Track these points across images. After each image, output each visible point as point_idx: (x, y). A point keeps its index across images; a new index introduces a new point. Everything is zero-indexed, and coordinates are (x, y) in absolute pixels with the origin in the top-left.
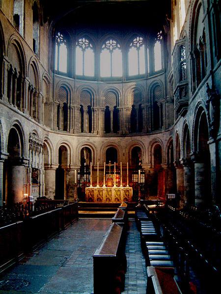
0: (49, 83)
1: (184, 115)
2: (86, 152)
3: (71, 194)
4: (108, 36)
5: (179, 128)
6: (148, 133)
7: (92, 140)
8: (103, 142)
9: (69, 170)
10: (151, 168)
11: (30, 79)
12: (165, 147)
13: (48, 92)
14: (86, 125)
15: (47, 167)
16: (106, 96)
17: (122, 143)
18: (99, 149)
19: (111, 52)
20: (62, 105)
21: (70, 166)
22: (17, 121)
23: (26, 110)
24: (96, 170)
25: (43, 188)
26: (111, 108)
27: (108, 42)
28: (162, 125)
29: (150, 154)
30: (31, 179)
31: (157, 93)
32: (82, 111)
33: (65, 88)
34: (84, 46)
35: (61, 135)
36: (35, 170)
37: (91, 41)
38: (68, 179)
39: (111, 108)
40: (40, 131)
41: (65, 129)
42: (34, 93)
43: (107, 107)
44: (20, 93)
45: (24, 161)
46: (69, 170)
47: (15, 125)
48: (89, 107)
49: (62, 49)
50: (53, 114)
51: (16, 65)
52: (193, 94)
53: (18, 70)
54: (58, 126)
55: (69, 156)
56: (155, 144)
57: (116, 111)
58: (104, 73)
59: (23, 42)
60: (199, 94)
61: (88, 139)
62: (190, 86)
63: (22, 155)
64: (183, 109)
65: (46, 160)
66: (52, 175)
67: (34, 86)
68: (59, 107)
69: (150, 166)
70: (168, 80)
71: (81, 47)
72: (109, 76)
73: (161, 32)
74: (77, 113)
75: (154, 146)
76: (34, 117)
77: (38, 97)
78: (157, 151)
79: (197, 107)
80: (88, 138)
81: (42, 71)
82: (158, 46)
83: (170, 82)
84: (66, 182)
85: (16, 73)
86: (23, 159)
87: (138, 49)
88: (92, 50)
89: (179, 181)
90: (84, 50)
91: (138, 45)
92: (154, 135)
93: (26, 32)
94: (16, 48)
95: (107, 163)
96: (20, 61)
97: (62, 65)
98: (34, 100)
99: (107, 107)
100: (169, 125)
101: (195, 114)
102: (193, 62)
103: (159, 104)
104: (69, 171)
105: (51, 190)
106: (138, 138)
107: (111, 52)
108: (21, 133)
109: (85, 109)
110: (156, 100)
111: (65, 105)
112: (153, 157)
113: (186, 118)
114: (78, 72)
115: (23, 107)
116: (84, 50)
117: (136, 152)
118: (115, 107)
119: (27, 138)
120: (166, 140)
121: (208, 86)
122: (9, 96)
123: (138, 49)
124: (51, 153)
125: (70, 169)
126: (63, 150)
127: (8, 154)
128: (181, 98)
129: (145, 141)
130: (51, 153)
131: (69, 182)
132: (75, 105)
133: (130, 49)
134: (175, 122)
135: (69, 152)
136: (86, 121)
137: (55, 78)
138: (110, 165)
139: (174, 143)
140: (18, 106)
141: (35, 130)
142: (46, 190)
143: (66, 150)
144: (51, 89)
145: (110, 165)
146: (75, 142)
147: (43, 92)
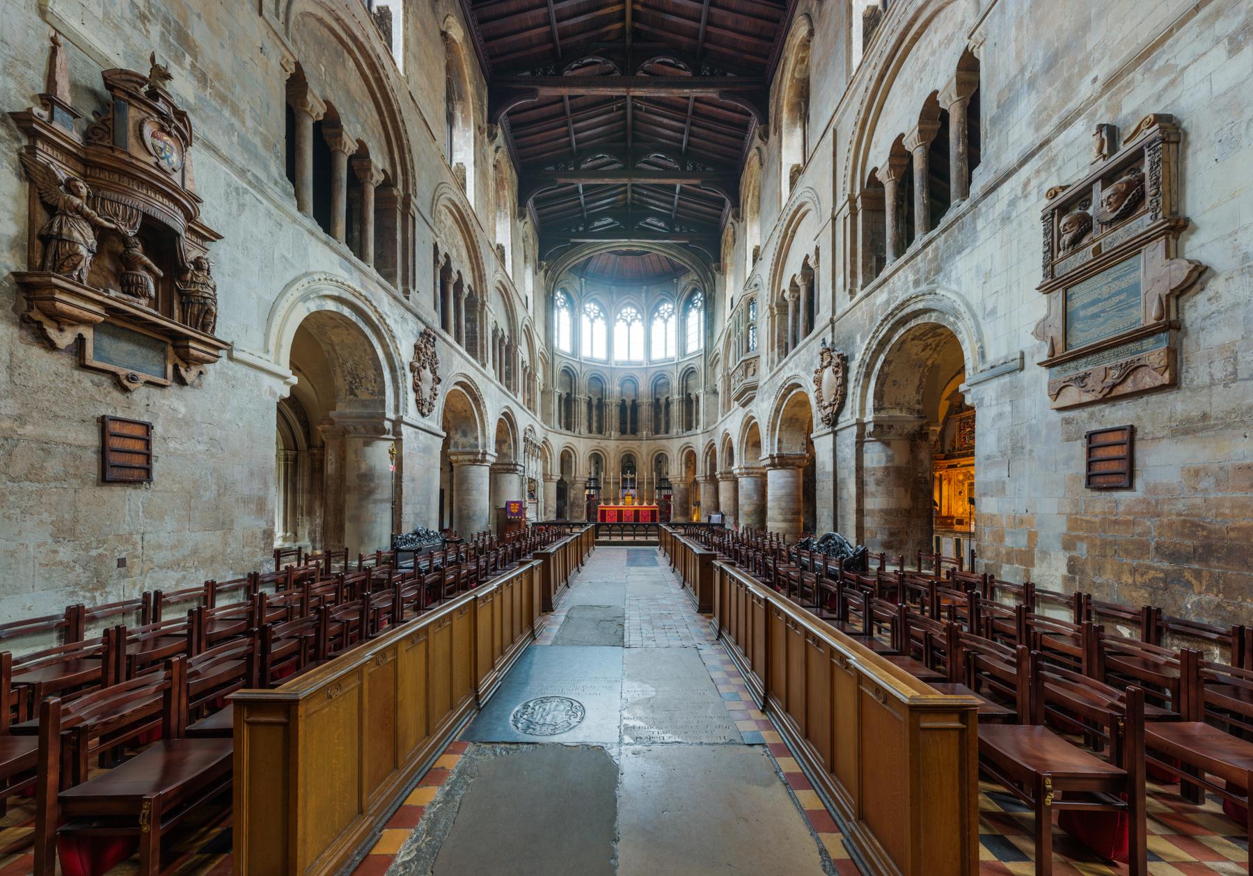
0: (547, 363)
1: (744, 405)
2: (597, 459)
4: (626, 301)
5: (732, 425)
7: (604, 443)
9: (574, 483)
11: (523, 352)
12: (701, 452)
13: (545, 376)
14: (595, 425)
15: (547, 477)
16: (622, 385)
17: (643, 449)
18: (612, 455)
19: (629, 325)
20: (564, 396)
22: (507, 407)
23: (520, 395)
24: (609, 483)
25: (541, 505)
26: (629, 402)
27: (624, 311)
28: (697, 423)
30: (527, 494)
31: (691, 382)
32: (589, 404)
33: (568, 373)
34: (592, 315)
36: (532, 481)
37: (602, 309)
38: (572, 495)
39: (629, 402)
40: (537, 428)
41: (568, 427)
42: (530, 376)
43: (624, 401)
44: (510, 370)
45: (518, 467)
47: (504, 414)
48: (600, 400)
49: (563, 318)
50: (555, 406)
51: (503, 325)
52: (771, 370)
53: (506, 333)
54: (560, 424)
57: (635, 406)
58: (620, 355)
59: (512, 289)
60: (791, 365)
62: (763, 358)
63: (515, 459)
64: (747, 395)
65: (545, 468)
66: (553, 488)
67: (528, 364)
68: (560, 397)
70: (708, 363)
71: (588, 315)
72: (625, 358)
73: (700, 295)
74: (584, 408)
76: (529, 408)
77: (534, 380)
78: (690, 457)
79: (782, 387)
81: (539, 345)
82: (695, 318)
83: (711, 365)
85: (503, 335)
86: (516, 464)
87: (666, 321)
88: (603, 322)
90: (592, 321)
91: (666, 315)
93: (516, 271)
94: (500, 291)
95: (624, 472)
96: (509, 319)
97: (563, 343)
98: (529, 384)
99: (624, 401)
100: (708, 424)
101: (776, 398)
102: (773, 321)
103: (693, 397)
105: (550, 509)
106: (664, 442)
107: (629, 325)
108: (513, 425)
109: (595, 402)
110: (689, 391)
111: (569, 395)
112: (684, 466)
113: (751, 406)
114: (585, 352)
115: (515, 390)
116: (592, 321)
117: (660, 460)
118: (634, 401)
119: (521, 435)
121: (824, 343)
122: (494, 367)
123: (666, 321)
125: (575, 480)
126: (566, 458)
127: (496, 455)
128: (746, 378)
129: (674, 447)
132: (582, 397)
133: (655, 322)
134: (720, 419)
136: (595, 418)
137: (555, 357)
138: (629, 476)
139: (718, 447)
140: (508, 387)
141: (531, 426)
142: (545, 508)
144: (550, 373)
145: (629, 476)
146: (583, 447)
147: (540, 375)
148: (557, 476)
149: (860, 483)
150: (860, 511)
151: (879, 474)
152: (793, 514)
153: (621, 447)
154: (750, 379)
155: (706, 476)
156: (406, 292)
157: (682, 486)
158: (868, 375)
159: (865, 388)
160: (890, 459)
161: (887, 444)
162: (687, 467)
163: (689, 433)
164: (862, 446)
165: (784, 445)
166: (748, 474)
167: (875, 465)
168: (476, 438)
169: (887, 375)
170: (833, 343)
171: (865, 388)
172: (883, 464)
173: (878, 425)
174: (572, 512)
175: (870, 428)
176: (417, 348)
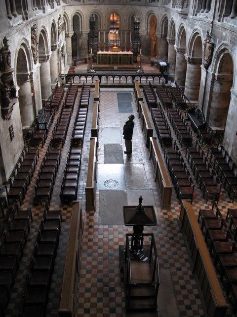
3: (83, 55)
6: (146, 5)
8: (107, 9)
10: (147, 34)
21: (81, 32)
29: (147, 22)
35: (75, 6)
38: (80, 43)
46: (81, 34)
55: (80, 23)
56: (151, 15)
61: (96, 7)
69: (146, 33)
75: (150, 16)
80: (95, 6)
84: (79, 44)
89: (170, 54)
92: (150, 7)
104: (81, 35)
106: (138, 7)
120: (161, 15)
124: (68, 24)
126: (76, 19)
129: (144, 10)
130: (68, 24)
131: (81, 44)
135: (80, 20)
143: (78, 18)
148: (71, 33)
149: (211, 96)
150: (209, 107)
151: (217, 95)
152: (196, 86)
153: (110, 9)
154: (185, 10)
155: (162, 35)
156: (26, 14)
157: (147, 37)
158: (218, 58)
159: (217, 62)
160: (222, 90)
161: (221, 84)
162: (151, 25)
163: (153, 4)
164: (214, 83)
165: (195, 53)
166: (181, 52)
167: (216, 91)
168: (44, 49)
169: (224, 60)
170: (211, 33)
171: (217, 62)
172: (219, 91)
173: (219, 78)
174: (80, 53)
175: (216, 78)
176: (32, 38)
